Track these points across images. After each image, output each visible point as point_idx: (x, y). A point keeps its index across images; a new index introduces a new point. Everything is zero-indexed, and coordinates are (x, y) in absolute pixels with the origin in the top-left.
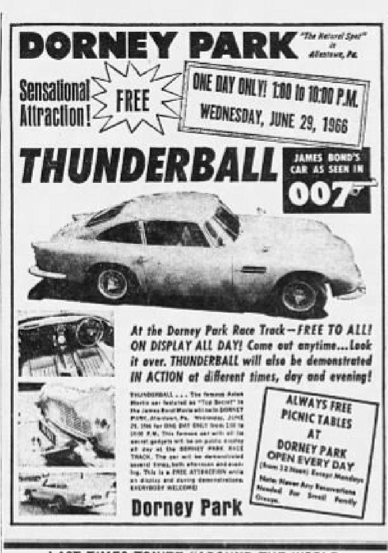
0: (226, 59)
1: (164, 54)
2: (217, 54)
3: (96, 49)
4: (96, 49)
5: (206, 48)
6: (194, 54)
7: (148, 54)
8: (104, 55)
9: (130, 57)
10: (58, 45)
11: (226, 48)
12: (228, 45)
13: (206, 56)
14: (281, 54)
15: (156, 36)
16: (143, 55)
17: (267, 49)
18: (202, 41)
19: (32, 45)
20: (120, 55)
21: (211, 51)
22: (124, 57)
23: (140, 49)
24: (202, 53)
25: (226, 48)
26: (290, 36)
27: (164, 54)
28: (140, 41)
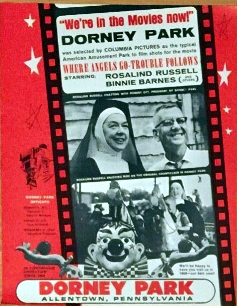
0: (155, 295)
1: (119, 292)
2: (150, 293)
3: (82, 290)
4: (82, 290)
5: (144, 289)
6: (138, 292)
7: (110, 292)
8: (86, 293)
9: (101, 294)
10: (61, 288)
11: (155, 289)
12: (156, 288)
13: (144, 294)
14: (185, 293)
15: (115, 284)
16: (108, 293)
17: (177, 290)
18: (142, 286)
19: (46, 288)
20: (95, 293)
21: (146, 292)
22: (97, 293)
23: (106, 290)
24: (142, 292)
25: (155, 289)
26: (189, 283)
27: (119, 292)
28: (106, 286)
